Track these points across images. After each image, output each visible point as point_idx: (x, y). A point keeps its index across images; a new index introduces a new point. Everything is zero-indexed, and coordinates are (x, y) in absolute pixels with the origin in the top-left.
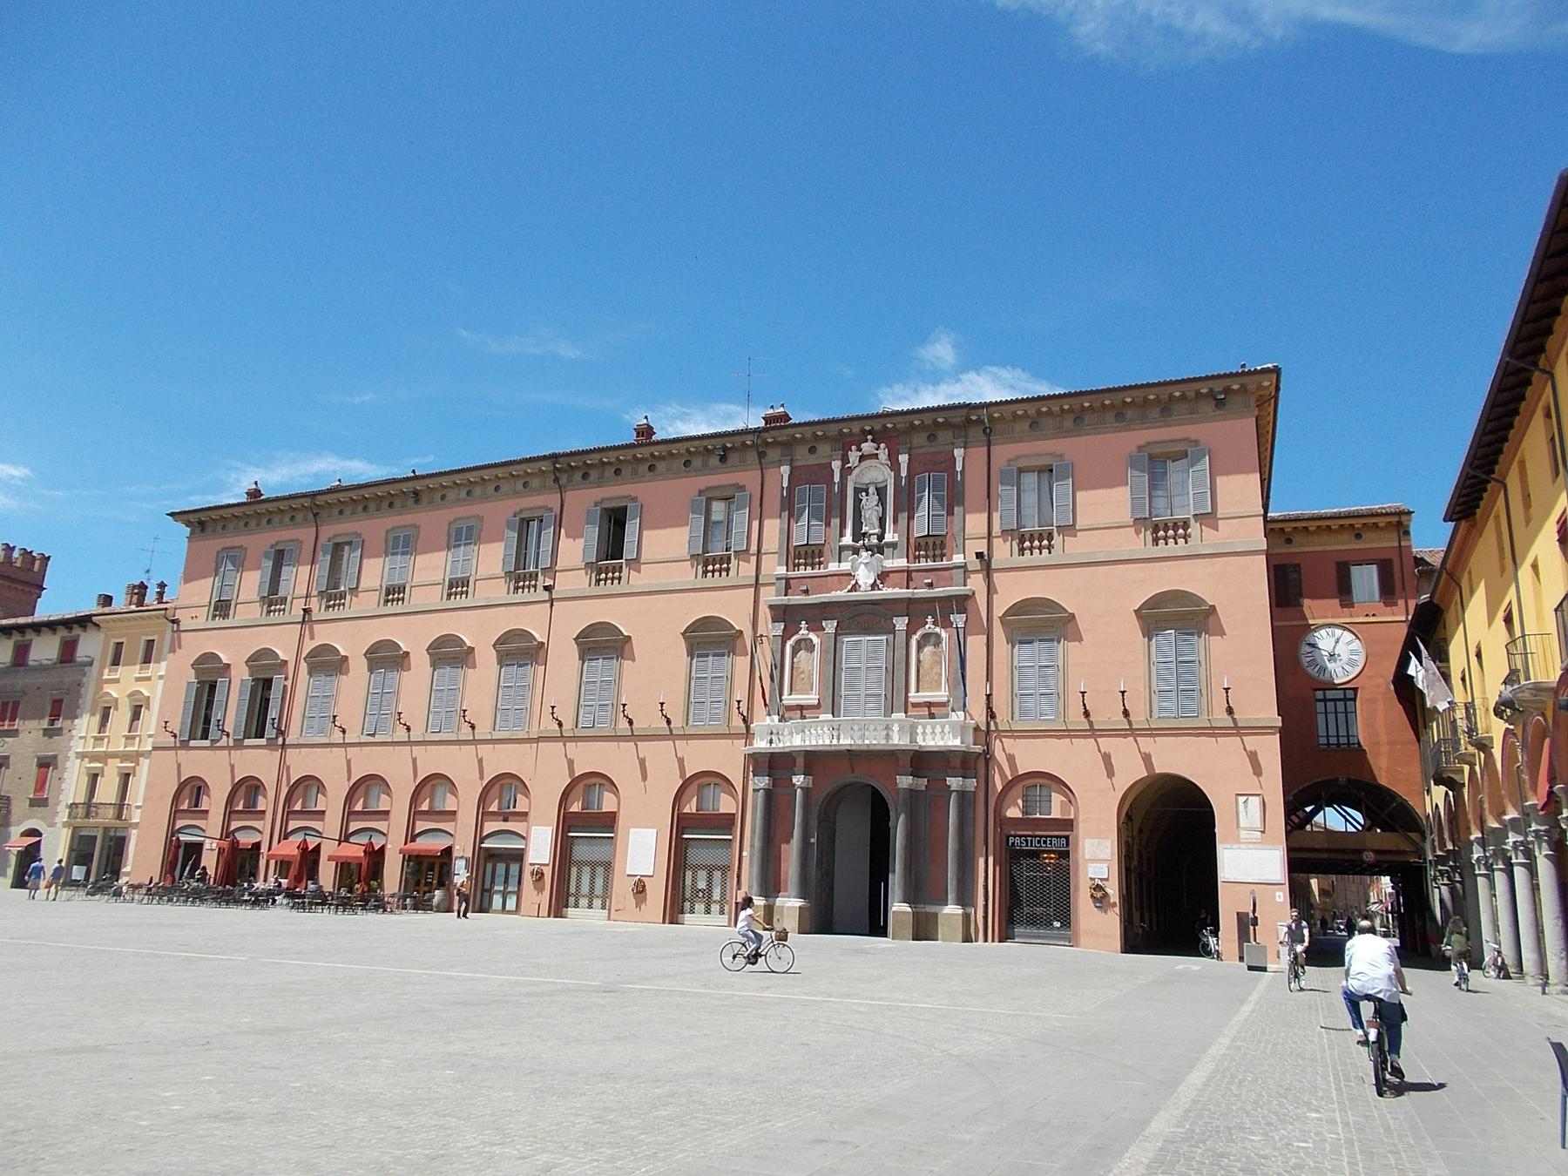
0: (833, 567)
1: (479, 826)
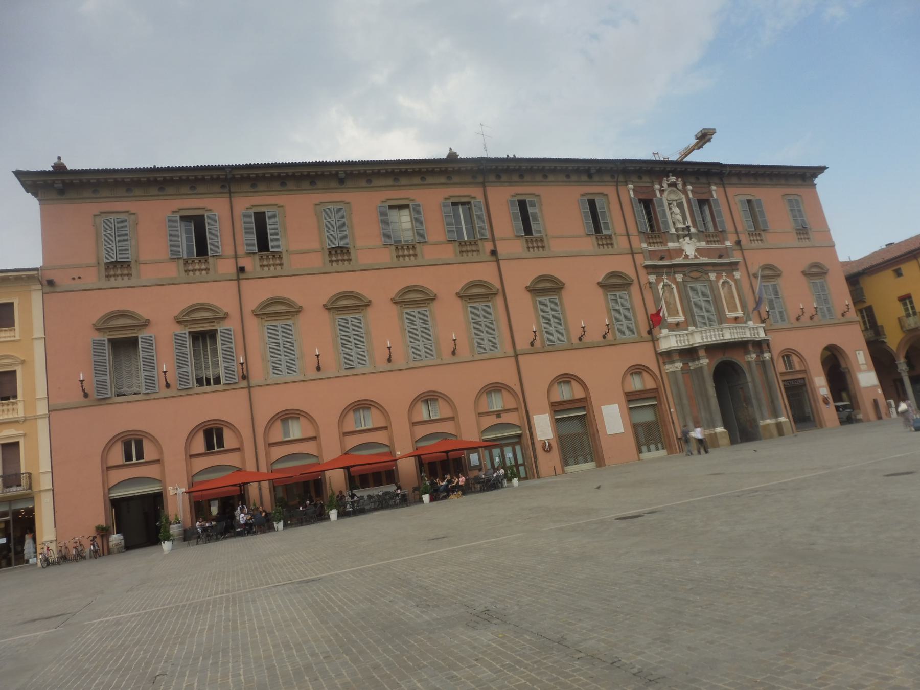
0: (671, 245)
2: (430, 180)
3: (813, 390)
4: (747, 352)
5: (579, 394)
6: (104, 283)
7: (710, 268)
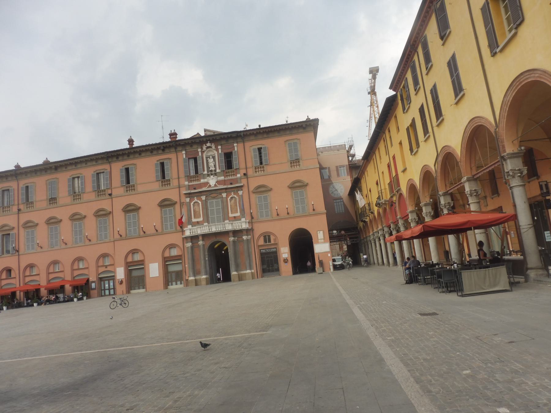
0: (202, 181)
1: (97, 270)
2: (89, 164)
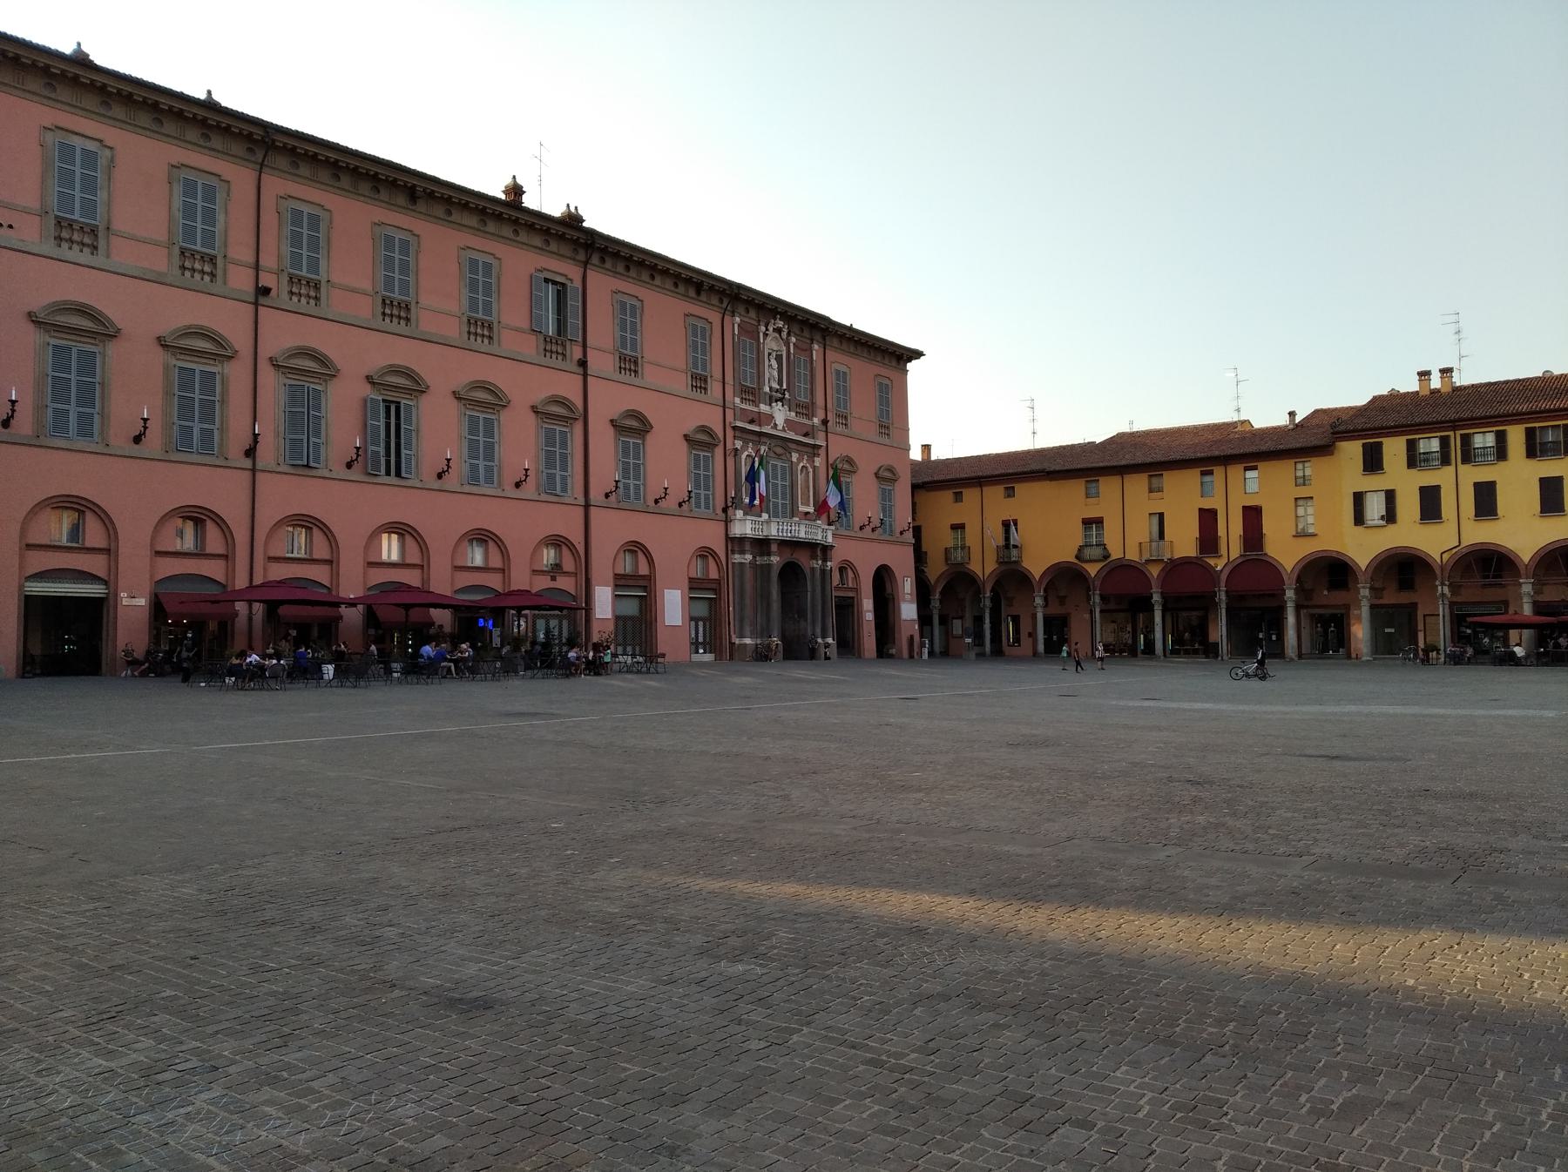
0: (764, 408)
3: (860, 613)
4: (814, 557)
5: (644, 570)
6: (49, 248)
7: (793, 446)
